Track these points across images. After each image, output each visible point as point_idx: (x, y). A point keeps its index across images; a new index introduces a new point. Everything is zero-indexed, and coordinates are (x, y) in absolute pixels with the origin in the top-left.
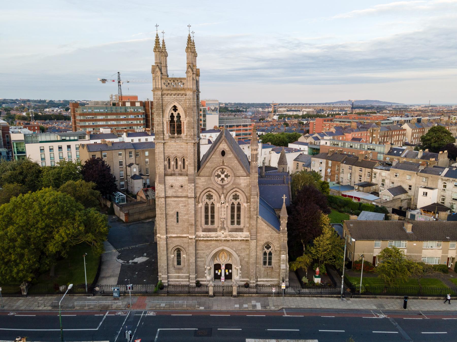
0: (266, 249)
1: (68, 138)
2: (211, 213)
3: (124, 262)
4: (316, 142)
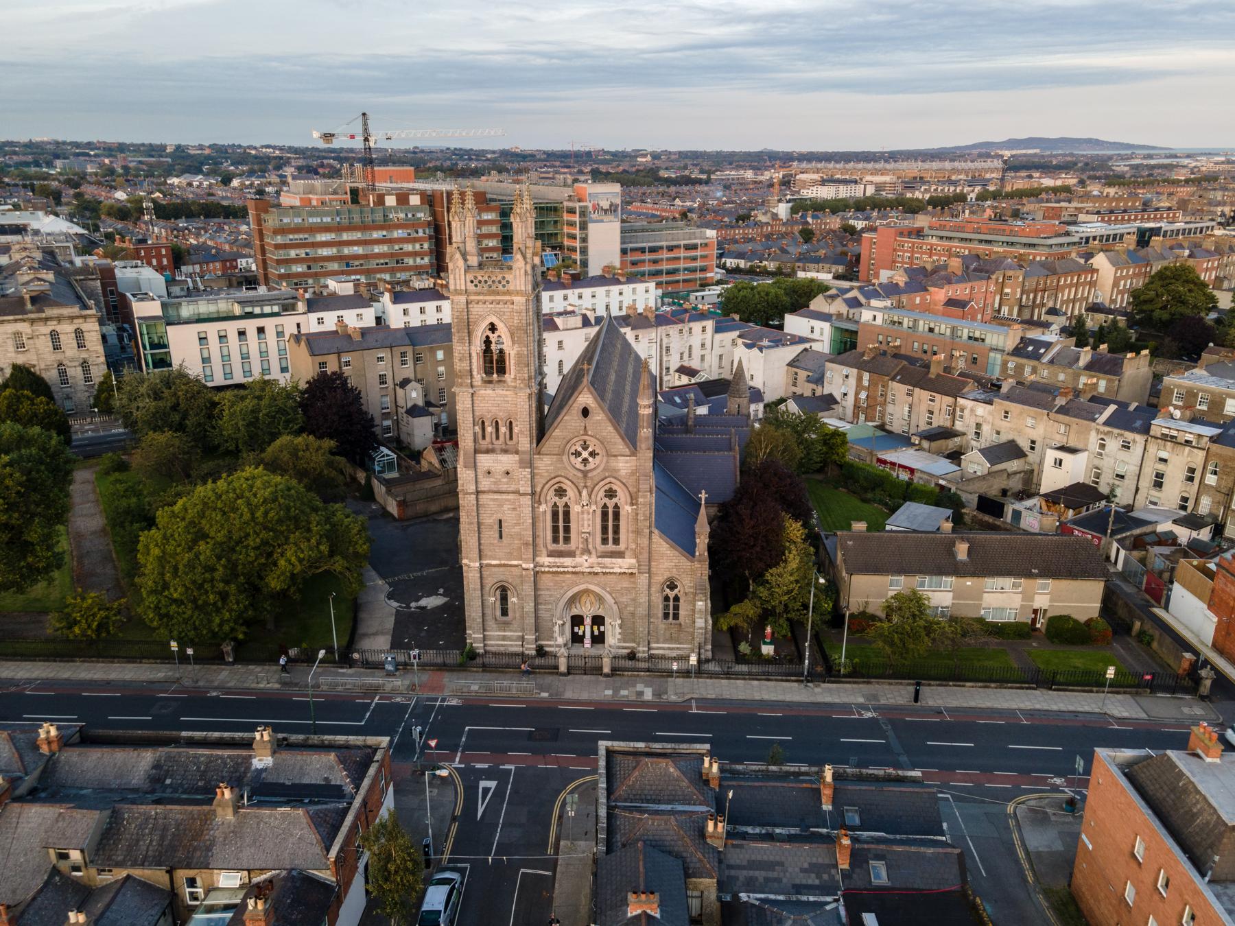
0: (668, 590)
1: (257, 310)
2: (564, 522)
4: (852, 311)
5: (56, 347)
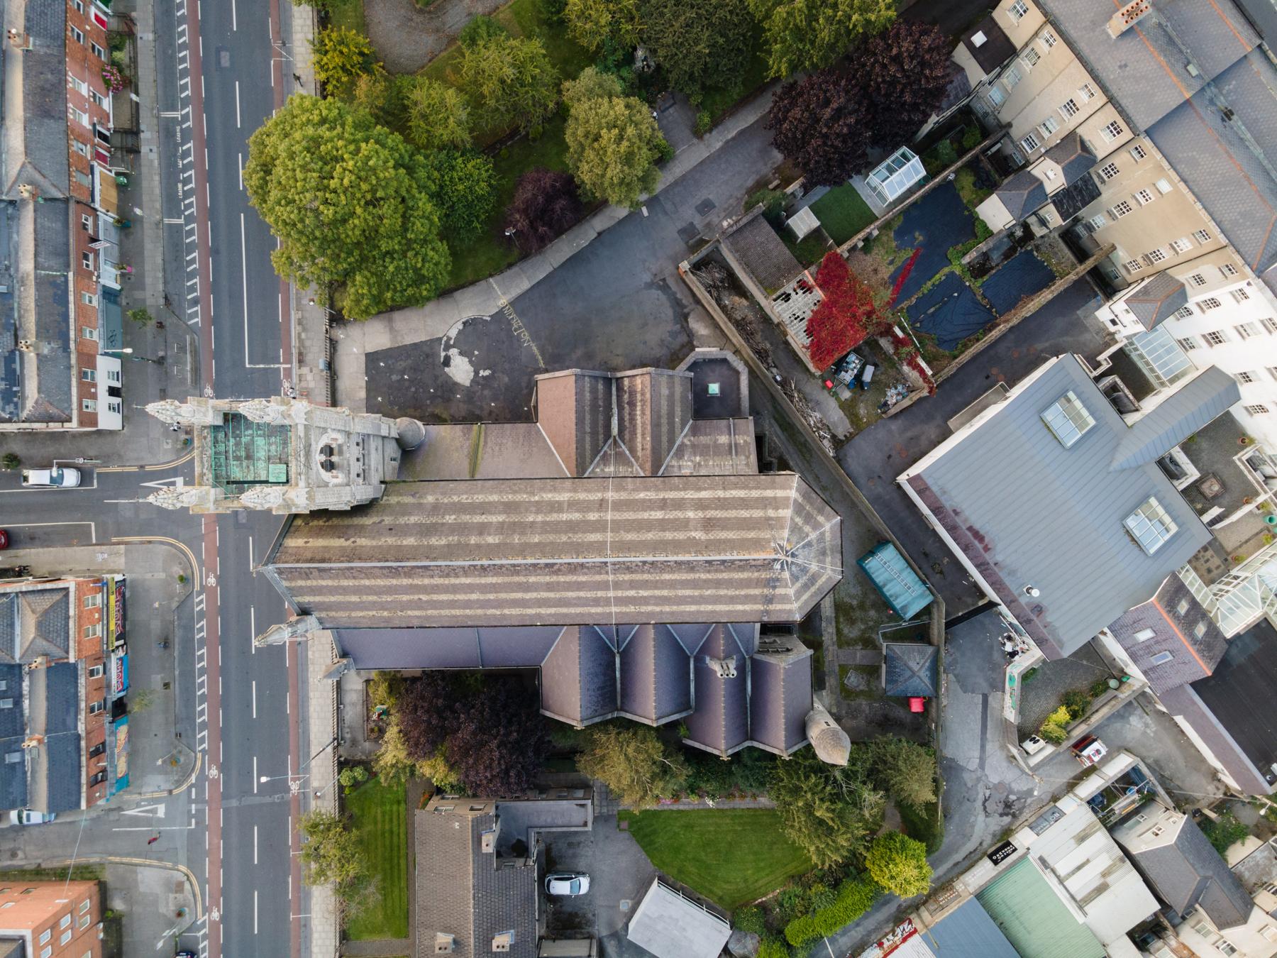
3: (449, 339)
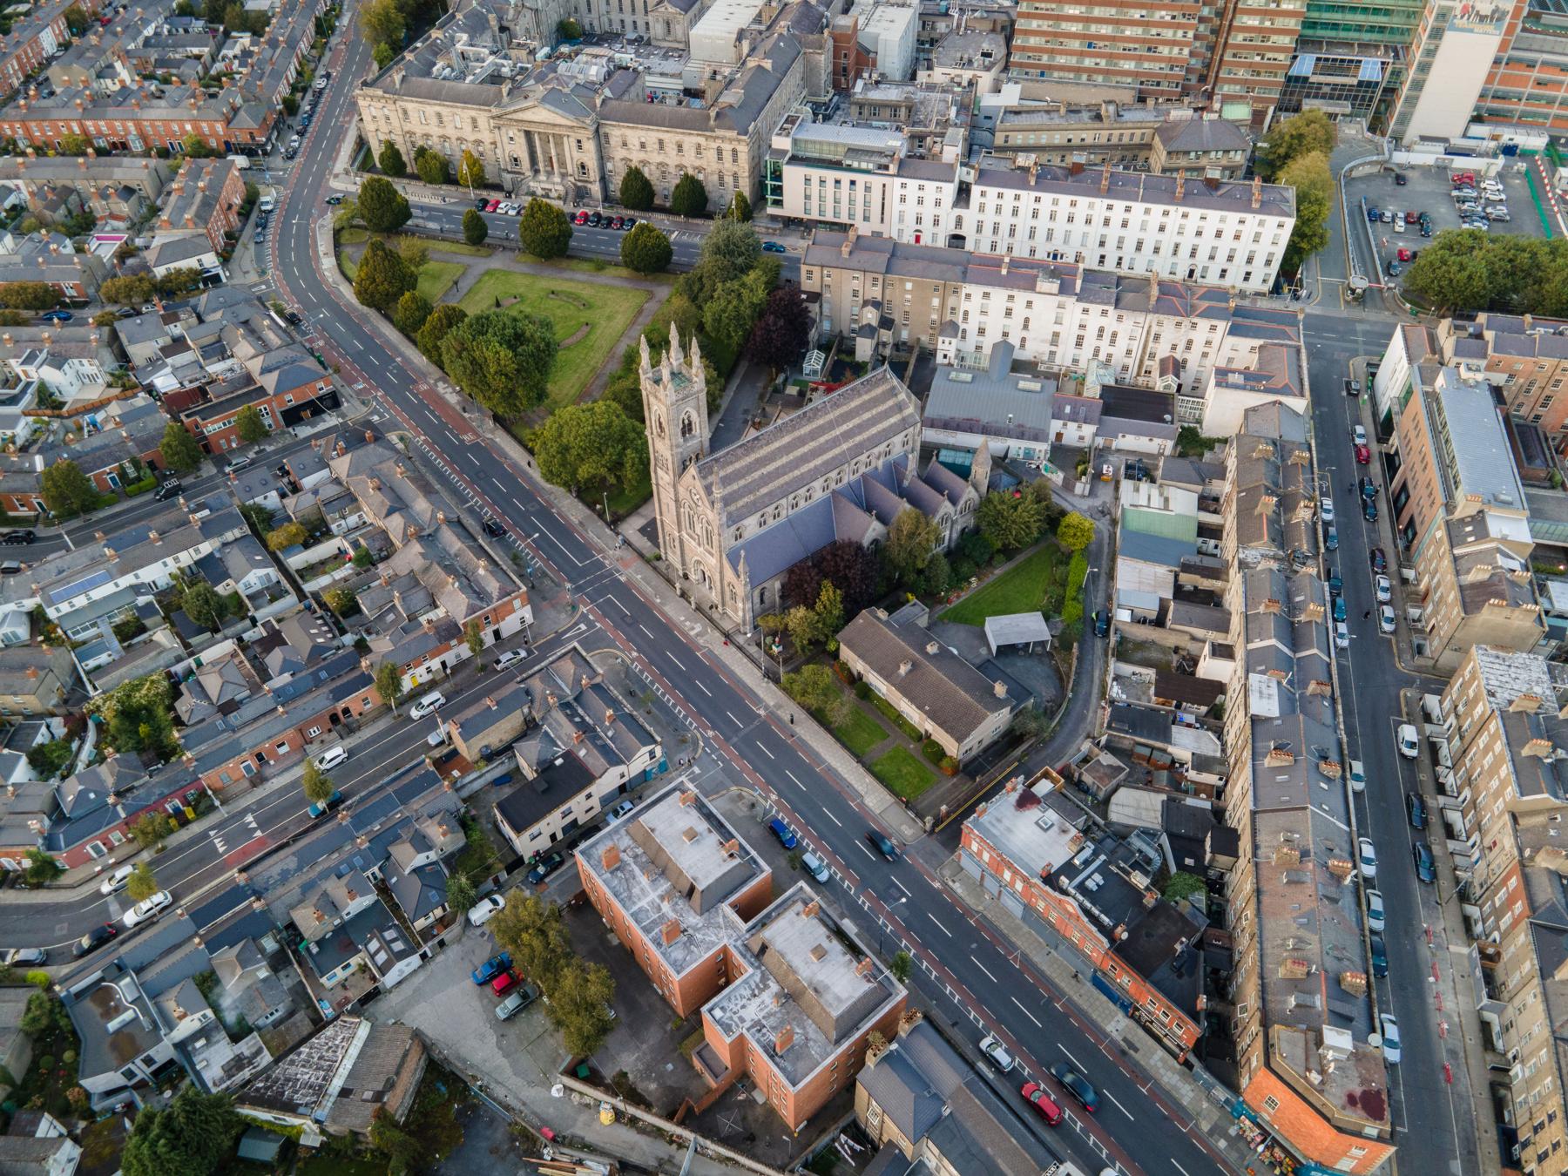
1: (855, 165)
5: (720, 159)
